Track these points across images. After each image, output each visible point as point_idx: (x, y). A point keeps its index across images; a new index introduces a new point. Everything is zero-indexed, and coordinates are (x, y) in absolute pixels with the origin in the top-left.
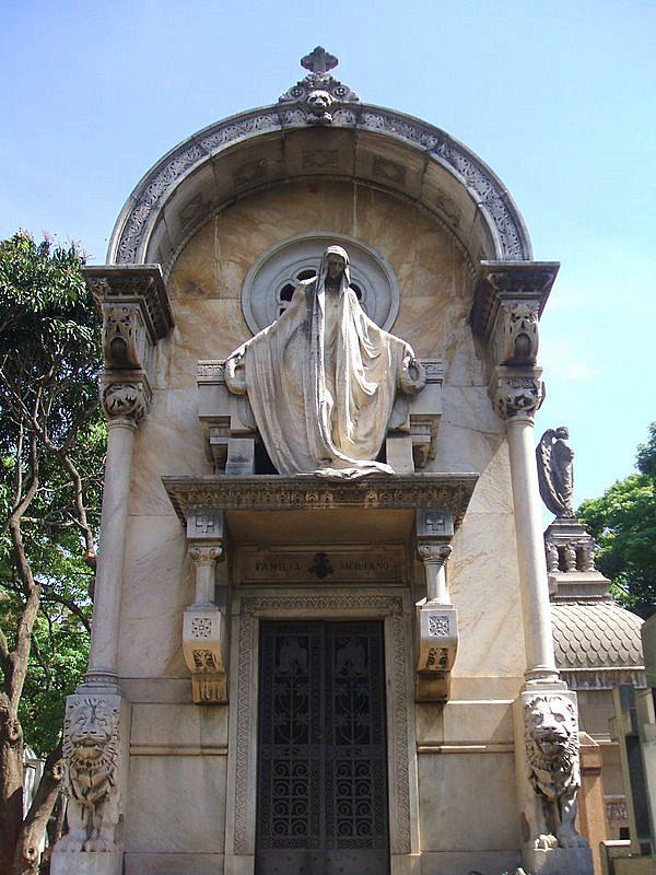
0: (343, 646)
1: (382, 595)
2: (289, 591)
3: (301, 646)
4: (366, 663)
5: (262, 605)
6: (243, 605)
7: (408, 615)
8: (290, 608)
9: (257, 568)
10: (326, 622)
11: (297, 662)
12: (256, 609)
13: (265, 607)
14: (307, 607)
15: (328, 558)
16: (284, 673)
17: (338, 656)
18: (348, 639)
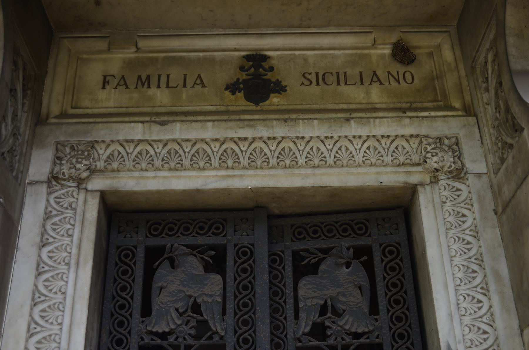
0: (313, 269)
1: (408, 131)
3: (208, 268)
4: (374, 310)
5: (110, 159)
6: (58, 158)
7: (479, 175)
8: (180, 167)
9: (105, 83)
10: (271, 217)
11: (196, 308)
12: (93, 171)
13: (115, 165)
14: (222, 164)
15: (274, 63)
16: (164, 336)
17: (301, 292)
18: (326, 251)
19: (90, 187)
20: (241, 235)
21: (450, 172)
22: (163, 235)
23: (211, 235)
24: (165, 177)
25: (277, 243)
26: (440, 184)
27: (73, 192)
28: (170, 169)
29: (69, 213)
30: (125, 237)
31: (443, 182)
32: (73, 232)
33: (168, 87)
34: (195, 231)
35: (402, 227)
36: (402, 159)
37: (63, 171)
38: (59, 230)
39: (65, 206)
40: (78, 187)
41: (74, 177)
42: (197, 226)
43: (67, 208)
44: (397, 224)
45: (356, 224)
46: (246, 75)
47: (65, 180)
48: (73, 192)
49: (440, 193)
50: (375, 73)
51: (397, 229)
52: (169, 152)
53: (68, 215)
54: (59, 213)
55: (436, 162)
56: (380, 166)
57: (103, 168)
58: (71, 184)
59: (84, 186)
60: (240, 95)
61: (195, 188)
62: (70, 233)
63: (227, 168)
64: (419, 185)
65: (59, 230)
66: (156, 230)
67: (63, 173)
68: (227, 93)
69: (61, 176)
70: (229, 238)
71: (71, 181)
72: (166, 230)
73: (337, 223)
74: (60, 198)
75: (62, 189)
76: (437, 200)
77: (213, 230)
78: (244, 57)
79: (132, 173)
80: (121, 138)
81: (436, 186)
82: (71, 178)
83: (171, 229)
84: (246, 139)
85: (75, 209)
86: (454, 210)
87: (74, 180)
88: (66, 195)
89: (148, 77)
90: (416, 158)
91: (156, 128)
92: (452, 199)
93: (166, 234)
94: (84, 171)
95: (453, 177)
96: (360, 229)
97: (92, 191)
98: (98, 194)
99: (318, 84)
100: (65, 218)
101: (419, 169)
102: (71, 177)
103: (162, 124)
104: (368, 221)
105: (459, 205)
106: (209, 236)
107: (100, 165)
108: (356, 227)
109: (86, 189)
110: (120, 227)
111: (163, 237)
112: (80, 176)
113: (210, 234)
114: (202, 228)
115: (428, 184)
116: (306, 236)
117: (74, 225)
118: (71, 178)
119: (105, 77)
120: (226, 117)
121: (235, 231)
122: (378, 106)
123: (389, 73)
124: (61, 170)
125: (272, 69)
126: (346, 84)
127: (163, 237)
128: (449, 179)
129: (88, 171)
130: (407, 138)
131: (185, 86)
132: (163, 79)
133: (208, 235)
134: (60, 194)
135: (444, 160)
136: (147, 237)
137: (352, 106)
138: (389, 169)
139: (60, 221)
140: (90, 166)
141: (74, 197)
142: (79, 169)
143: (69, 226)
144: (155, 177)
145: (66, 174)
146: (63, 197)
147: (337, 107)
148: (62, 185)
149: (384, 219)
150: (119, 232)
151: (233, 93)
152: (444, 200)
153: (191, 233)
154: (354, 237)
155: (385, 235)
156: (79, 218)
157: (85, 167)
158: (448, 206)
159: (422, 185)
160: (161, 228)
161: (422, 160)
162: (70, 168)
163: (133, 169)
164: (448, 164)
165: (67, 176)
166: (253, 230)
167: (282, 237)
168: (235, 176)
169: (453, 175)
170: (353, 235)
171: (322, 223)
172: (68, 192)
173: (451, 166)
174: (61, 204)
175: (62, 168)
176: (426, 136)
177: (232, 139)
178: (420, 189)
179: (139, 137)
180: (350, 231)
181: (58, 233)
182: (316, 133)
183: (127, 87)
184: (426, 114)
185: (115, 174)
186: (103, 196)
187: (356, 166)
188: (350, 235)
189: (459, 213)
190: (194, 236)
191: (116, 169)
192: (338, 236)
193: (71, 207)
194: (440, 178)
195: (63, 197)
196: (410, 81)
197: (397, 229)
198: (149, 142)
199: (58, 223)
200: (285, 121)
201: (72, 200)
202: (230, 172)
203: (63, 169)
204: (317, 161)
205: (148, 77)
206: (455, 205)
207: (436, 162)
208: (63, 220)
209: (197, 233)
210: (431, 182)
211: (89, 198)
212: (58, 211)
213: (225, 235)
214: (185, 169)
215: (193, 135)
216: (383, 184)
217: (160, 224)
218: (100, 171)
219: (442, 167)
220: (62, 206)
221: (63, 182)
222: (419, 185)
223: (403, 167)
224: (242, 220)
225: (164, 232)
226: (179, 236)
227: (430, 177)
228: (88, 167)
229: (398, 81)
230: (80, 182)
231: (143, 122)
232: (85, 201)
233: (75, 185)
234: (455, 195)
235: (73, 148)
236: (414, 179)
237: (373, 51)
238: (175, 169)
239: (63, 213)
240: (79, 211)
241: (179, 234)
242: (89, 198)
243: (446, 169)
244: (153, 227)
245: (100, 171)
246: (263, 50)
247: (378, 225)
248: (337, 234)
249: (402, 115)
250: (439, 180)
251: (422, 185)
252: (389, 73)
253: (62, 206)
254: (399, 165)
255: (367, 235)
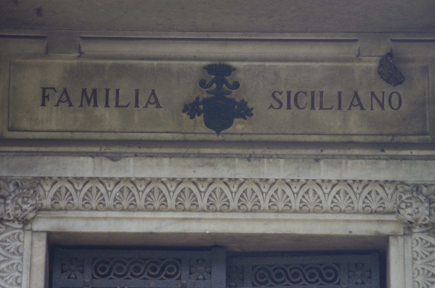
1: (382, 176)
2: (131, 161)
9: (45, 98)
12: (38, 209)
15: (239, 76)
19: (35, 228)
20: (197, 279)
21: (426, 225)
22: (111, 276)
23: (164, 278)
24: (116, 218)
25: (236, 287)
26: (413, 237)
27: (19, 235)
28: (123, 210)
29: (16, 259)
30: (69, 278)
31: (417, 236)
32: (22, 281)
33: (117, 105)
34: (146, 273)
35: (376, 277)
36: (374, 206)
37: (7, 212)
38: (7, 278)
39: (12, 250)
40: (23, 228)
41: (20, 219)
42: (149, 267)
43: (13, 253)
44: (370, 271)
45: (325, 269)
46: (208, 92)
47: (9, 221)
48: (19, 235)
49: (412, 248)
50: (356, 95)
51: (370, 277)
52: (121, 191)
53: (16, 261)
54: (6, 259)
55: (409, 214)
56: (350, 213)
57: (49, 207)
58: (16, 225)
59: (29, 227)
60: (200, 119)
61: (149, 231)
62: (19, 281)
63: (184, 210)
64: (392, 236)
65: (7, 278)
66: (103, 269)
67: (9, 214)
68: (185, 116)
69: (5, 217)
70: (184, 282)
71: (16, 222)
72: (114, 271)
73: (303, 266)
74: (6, 242)
75: (7, 231)
76: (408, 255)
77: (166, 271)
78: (205, 68)
79: (81, 212)
80: (70, 175)
81: (409, 240)
82: (16, 219)
83: (120, 269)
84: (205, 179)
85: (21, 254)
86: (423, 269)
87: (19, 221)
88: (11, 238)
89: (94, 91)
90: (389, 206)
91: (107, 163)
92: (424, 256)
93: (115, 275)
94: (30, 212)
95: (428, 231)
96: (329, 275)
97: (37, 232)
98: (44, 236)
99: (289, 107)
100: (13, 264)
101: (393, 217)
102: (17, 219)
103: (114, 158)
104: (338, 265)
105: (430, 263)
106: (162, 279)
107: (47, 203)
108: (324, 273)
109: (31, 230)
110: (63, 265)
111: (111, 278)
112: (25, 218)
113: (162, 276)
114: (154, 269)
115: (401, 236)
116: (269, 280)
117: (21, 272)
118: (16, 219)
119: (44, 89)
120: (183, 150)
121: (191, 273)
122: (355, 139)
123: (373, 94)
124: (5, 211)
125: (236, 85)
126: (321, 108)
127: (111, 278)
128: (422, 232)
129: (35, 211)
130: (382, 184)
131: (137, 106)
132: (112, 95)
133: (160, 277)
134: (5, 238)
135: (418, 212)
136: (93, 277)
137: (326, 139)
138: (360, 217)
139: (8, 267)
140: (36, 205)
141: (20, 241)
142: (26, 210)
143: (17, 274)
144: (105, 218)
145: (11, 215)
146: (8, 240)
147: (308, 139)
148: (7, 227)
149: (356, 265)
150: (63, 272)
151: (192, 117)
152: (415, 256)
153: (143, 274)
154: (321, 284)
155: (357, 283)
156: (26, 264)
157: (32, 208)
158: (419, 264)
159: (395, 235)
160: (108, 268)
161: (396, 210)
162: (16, 209)
163: (82, 208)
164: (423, 217)
165: (12, 218)
166: (210, 273)
167: (243, 280)
168: (192, 219)
169: (428, 228)
170: (321, 281)
171: (287, 266)
172: (14, 234)
173: (425, 219)
174: (7, 248)
175: (7, 208)
176: (402, 183)
177: (190, 180)
178: (392, 240)
179: (89, 174)
180: (317, 277)
181: (6, 281)
182: (282, 175)
183: (70, 105)
184: (407, 153)
185: (62, 214)
186: (50, 235)
187: (324, 213)
188: (317, 281)
189: (428, 272)
190: (145, 278)
191: (63, 208)
192: (304, 282)
193: (18, 252)
194: (414, 230)
195: (8, 240)
196: (395, 106)
197: (370, 277)
198: (101, 181)
199: (6, 270)
200: (249, 158)
201: (19, 244)
202: (187, 215)
203: (8, 210)
204: (281, 206)
205: (94, 91)
206: (426, 263)
207: (409, 214)
208: (10, 267)
209: (149, 274)
210: (405, 234)
211: (35, 240)
212: (5, 257)
213: (179, 278)
214: (139, 210)
215: (148, 174)
216: (353, 233)
217: (107, 263)
218: (47, 210)
219: (416, 220)
220: (8, 250)
221: (7, 224)
222: (392, 236)
223: (375, 215)
224: (198, 261)
225: (112, 273)
226: (128, 278)
227: (404, 228)
228: (34, 207)
229: (382, 106)
230: (25, 222)
231: (92, 155)
232: (32, 244)
233: (20, 226)
234: (428, 251)
235: (17, 185)
236: (386, 229)
237: (357, 64)
238: (128, 210)
239: (10, 259)
240: (26, 255)
241: (128, 275)
242: (35, 240)
243: (420, 222)
244: (100, 266)
245: (47, 210)
246: (226, 60)
247: (349, 271)
248: (303, 279)
249: (379, 153)
250: (413, 233)
251: (395, 235)
252: (373, 94)
253: (8, 250)
254: (371, 213)
255: (336, 282)
